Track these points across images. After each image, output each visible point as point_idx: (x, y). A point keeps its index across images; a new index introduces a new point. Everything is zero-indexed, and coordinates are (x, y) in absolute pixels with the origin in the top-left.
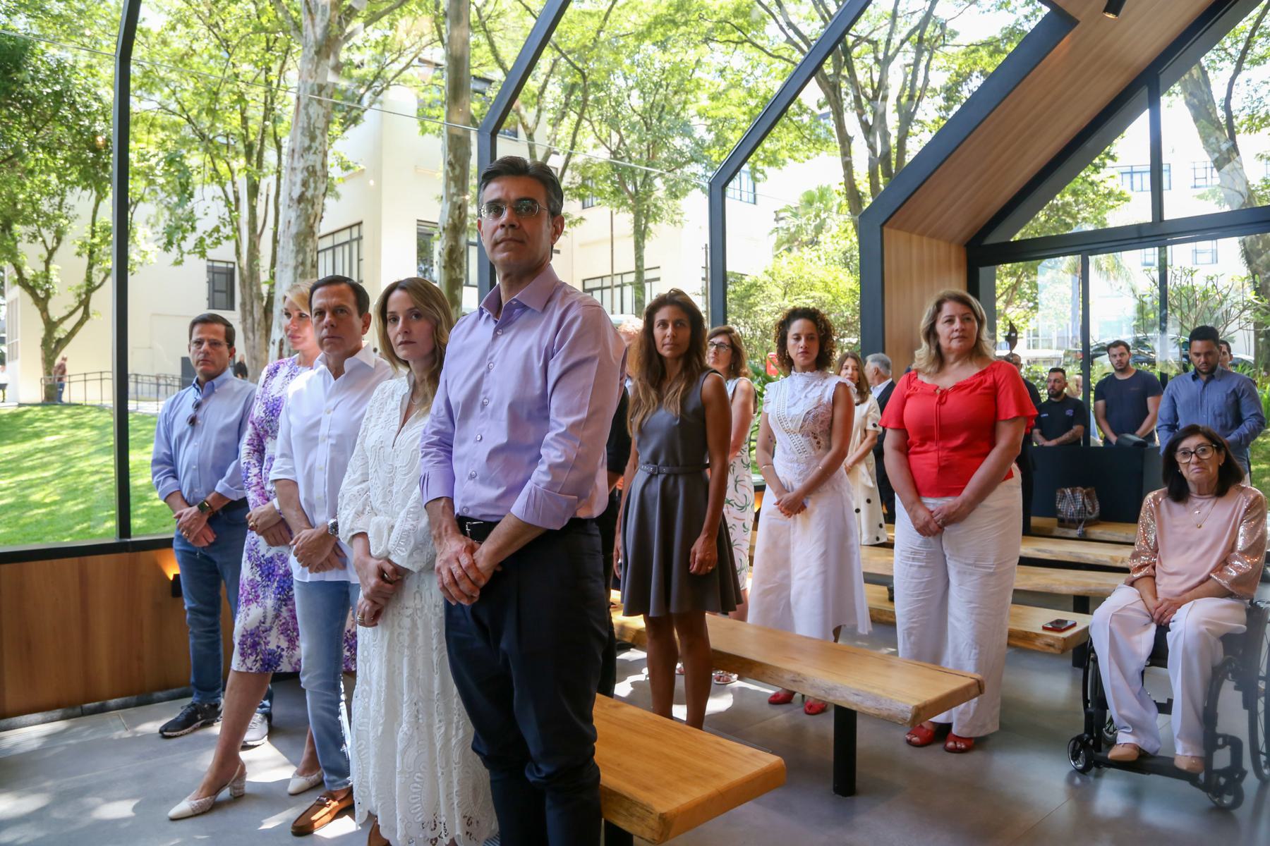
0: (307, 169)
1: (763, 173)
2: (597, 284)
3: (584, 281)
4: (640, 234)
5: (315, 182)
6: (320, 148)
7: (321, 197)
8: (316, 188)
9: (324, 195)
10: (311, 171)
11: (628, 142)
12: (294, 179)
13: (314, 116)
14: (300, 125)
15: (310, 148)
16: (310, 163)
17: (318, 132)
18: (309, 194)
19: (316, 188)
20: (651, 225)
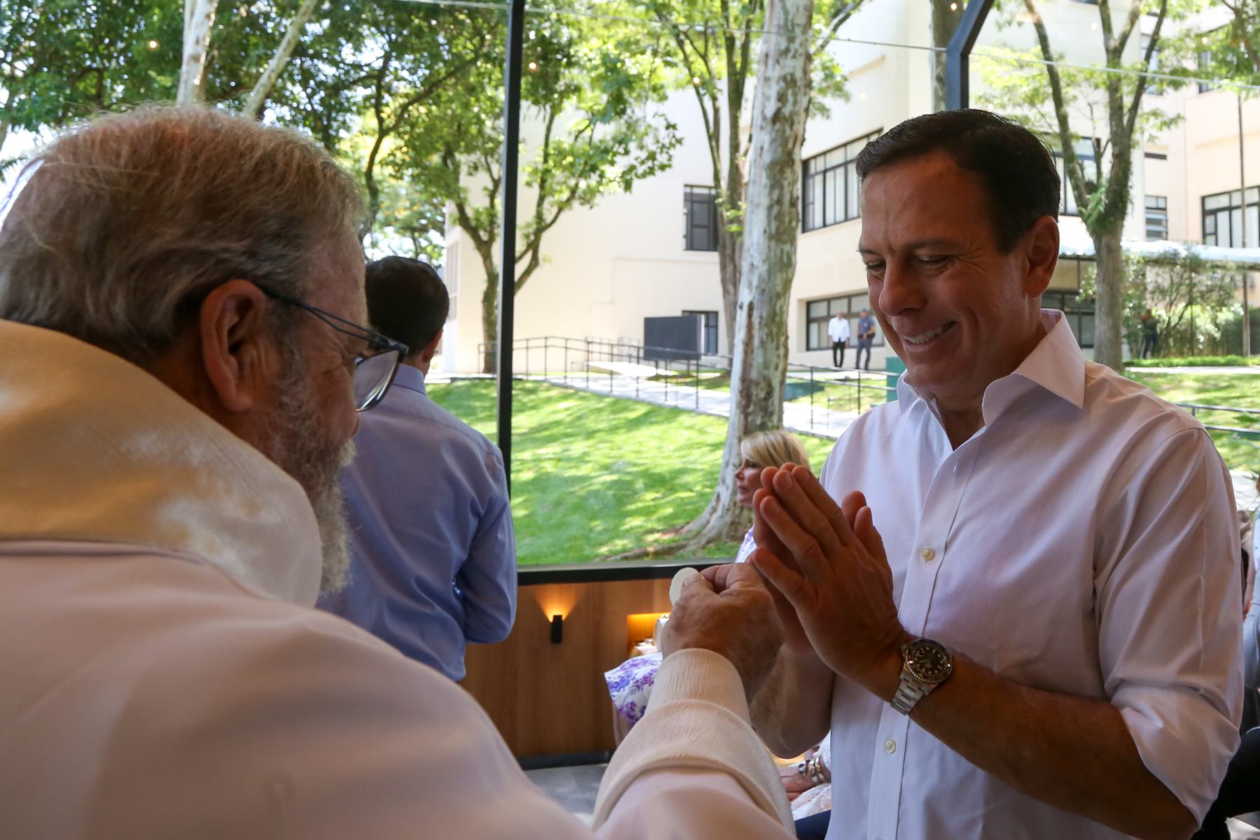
0: (784, 78)
2: (1224, 202)
3: (1203, 199)
5: (795, 95)
6: (801, 50)
7: (803, 115)
10: (789, 81)
12: (768, 92)
14: (775, 22)
15: (787, 51)
16: (788, 70)
18: (787, 111)
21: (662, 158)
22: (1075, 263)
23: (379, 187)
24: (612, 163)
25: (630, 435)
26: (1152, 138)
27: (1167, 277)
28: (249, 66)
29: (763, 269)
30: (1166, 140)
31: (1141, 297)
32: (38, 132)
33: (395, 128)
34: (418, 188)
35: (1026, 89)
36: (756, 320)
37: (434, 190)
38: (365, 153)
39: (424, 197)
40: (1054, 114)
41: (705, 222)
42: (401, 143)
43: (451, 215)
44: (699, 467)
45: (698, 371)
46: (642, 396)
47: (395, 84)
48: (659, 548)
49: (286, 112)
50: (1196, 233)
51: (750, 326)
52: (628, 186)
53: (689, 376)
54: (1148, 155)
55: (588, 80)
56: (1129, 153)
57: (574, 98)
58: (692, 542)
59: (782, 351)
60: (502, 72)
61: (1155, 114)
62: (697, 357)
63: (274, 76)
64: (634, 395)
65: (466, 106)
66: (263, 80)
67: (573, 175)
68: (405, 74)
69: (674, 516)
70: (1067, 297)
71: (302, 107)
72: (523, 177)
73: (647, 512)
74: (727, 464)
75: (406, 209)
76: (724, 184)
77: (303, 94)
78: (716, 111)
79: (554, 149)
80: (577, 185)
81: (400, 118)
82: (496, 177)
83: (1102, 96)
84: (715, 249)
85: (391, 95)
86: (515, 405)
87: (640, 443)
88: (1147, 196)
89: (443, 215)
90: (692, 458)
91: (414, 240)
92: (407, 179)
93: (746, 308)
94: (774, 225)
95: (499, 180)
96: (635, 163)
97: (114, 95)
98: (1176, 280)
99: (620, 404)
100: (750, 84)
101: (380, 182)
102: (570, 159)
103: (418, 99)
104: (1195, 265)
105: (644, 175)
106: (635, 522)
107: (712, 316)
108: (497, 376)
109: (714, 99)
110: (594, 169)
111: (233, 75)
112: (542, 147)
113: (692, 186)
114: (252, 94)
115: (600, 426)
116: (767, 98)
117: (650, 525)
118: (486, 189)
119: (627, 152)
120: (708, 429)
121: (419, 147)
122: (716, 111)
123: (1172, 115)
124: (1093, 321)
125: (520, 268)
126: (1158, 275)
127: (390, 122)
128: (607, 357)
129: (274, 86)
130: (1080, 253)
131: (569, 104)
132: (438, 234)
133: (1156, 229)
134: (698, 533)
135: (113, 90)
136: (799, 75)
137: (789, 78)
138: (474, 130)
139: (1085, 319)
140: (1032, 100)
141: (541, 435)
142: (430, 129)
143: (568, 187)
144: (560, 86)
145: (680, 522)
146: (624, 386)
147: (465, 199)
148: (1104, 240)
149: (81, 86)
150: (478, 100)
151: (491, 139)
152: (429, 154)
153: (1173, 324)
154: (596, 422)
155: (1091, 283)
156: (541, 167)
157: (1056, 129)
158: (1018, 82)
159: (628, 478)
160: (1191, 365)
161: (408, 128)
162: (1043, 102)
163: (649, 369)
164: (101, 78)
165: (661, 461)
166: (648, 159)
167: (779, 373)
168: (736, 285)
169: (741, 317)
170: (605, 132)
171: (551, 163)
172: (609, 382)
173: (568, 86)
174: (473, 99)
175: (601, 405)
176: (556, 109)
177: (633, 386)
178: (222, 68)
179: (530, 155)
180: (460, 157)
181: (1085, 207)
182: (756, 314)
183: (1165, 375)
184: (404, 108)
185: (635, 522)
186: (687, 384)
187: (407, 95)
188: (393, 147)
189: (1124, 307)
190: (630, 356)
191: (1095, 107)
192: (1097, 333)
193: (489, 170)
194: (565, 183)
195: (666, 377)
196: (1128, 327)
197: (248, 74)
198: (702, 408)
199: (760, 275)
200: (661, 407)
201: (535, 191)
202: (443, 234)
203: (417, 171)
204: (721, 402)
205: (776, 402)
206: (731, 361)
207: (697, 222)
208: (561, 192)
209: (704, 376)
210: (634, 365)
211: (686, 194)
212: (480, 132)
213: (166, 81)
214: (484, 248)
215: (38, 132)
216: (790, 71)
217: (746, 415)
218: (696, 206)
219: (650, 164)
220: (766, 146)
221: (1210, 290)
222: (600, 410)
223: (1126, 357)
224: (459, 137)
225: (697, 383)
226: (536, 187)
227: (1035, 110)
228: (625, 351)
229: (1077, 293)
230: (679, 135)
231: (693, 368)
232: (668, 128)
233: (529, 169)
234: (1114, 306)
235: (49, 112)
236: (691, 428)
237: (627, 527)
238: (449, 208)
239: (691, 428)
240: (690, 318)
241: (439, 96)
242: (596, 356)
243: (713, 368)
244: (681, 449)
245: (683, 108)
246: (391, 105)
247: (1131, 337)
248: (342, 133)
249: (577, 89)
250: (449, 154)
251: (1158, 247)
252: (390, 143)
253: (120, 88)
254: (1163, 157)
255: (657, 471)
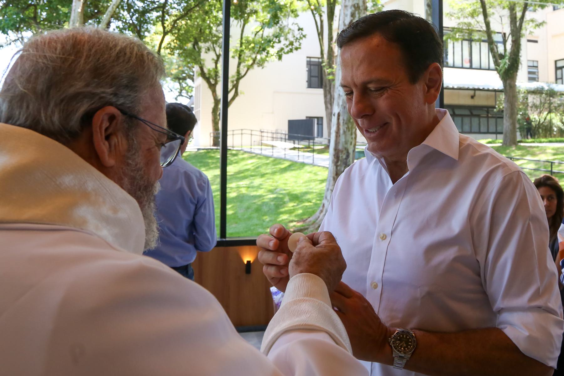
0: (354, 6)
3: (556, 62)
12: (346, 13)
21: (296, 44)
22: (494, 93)
23: (164, 59)
24: (273, 47)
25: (282, 175)
26: (531, 33)
27: (539, 99)
28: (103, 3)
30: (538, 33)
31: (526, 109)
32: (8, 34)
33: (171, 31)
34: (181, 59)
35: (470, 10)
36: (341, 121)
37: (189, 60)
38: (157, 43)
39: (184, 63)
40: (483, 21)
41: (317, 75)
42: (173, 38)
43: (197, 72)
44: (314, 191)
45: (313, 145)
46: (287, 157)
47: (171, 10)
48: (296, 229)
49: (120, 24)
50: (553, 78)
51: (338, 124)
52: (280, 58)
53: (309, 148)
54: (529, 41)
55: (261, 7)
56: (520, 40)
57: (254, 16)
58: (311, 227)
59: (353, 136)
60: (221, 4)
61: (532, 21)
62: (313, 139)
63: (115, 7)
64: (283, 157)
65: (204, 20)
66: (110, 9)
67: (254, 52)
68: (175, 6)
69: (303, 214)
70: (490, 109)
71: (127, 22)
72: (231, 54)
73: (290, 212)
74: (328, 189)
75: (176, 69)
76: (325, 56)
77: (128, 16)
78: (322, 22)
79: (245, 40)
80: (256, 57)
81: (173, 27)
82: (218, 54)
83: (506, 12)
84: (321, 87)
85: (169, 16)
86: (228, 161)
87: (286, 179)
88: (528, 60)
89: (193, 72)
90: (311, 187)
91: (180, 84)
92: (176, 55)
95: (220, 55)
96: (283, 47)
97: (42, 17)
98: (543, 101)
99: (277, 161)
100: (338, 9)
101: (164, 56)
102: (252, 45)
103: (181, 17)
104: (552, 94)
105: (288, 52)
106: (284, 217)
107: (320, 119)
108: (220, 148)
109: (321, 16)
110: (264, 50)
111: (96, 7)
112: (240, 40)
113: (310, 58)
114: (105, 16)
115: (268, 171)
116: (346, 15)
117: (291, 219)
118: (213, 59)
119: (280, 42)
120: (318, 173)
121: (182, 39)
122: (322, 22)
123: (540, 21)
124: (503, 121)
125: (230, 96)
126: (534, 98)
127: (168, 28)
128: (270, 139)
129: (115, 12)
130: (496, 88)
131: (252, 19)
132: (191, 81)
133: (533, 76)
134: (314, 223)
135: (41, 14)
136: (361, 4)
137: (356, 5)
138: (207, 31)
139: (499, 120)
140: (473, 15)
141: (241, 175)
142: (187, 31)
143: (252, 58)
144: (248, 10)
145: (305, 217)
146: (279, 152)
147: (204, 64)
148: (508, 82)
149: (27, 13)
150: (209, 18)
151: (215, 36)
152: (186, 43)
153: (541, 122)
154: (265, 169)
155: (502, 103)
156: (239, 49)
157: (484, 28)
158: (466, 6)
159: (281, 196)
160: (550, 142)
161: (177, 31)
162: (478, 16)
163: (290, 145)
164: (36, 9)
165: (296, 188)
166: (289, 45)
167: (352, 146)
168: (331, 104)
169: (334, 120)
170: (269, 32)
171: (244, 47)
172: (271, 150)
173: (251, 11)
174: (207, 17)
175: (268, 162)
176: (246, 21)
177: (283, 152)
178: (91, 3)
179: (234, 43)
180: (201, 44)
181: (499, 66)
182: (341, 118)
183: (538, 147)
184: (175, 22)
185: (284, 217)
186: (308, 151)
187: (176, 16)
188: (170, 40)
189: (517, 114)
190: (281, 138)
191: (503, 18)
192: (505, 126)
193: (215, 50)
194: (250, 56)
195: (299, 148)
196: (519, 124)
197: (103, 6)
198: (316, 163)
199: (343, 100)
200: (296, 162)
201: (236, 60)
202: (193, 80)
203: (181, 51)
204: (324, 160)
205: (351, 160)
206: (329, 141)
207: (312, 74)
208: (248, 60)
209: (317, 148)
210: (283, 142)
211: (307, 61)
212: (210, 32)
213: (65, 10)
214: (213, 87)
215: (8, 34)
216: (357, 2)
217: (337, 166)
218: (312, 67)
219: (290, 47)
221: (560, 106)
222: (267, 164)
223: (519, 138)
224: (201, 35)
225: (313, 151)
226: (237, 58)
227: (474, 20)
228: (279, 136)
229: (495, 108)
230: (304, 33)
231: (311, 144)
232: (299, 29)
233: (233, 50)
234: (513, 114)
235: (12, 25)
236: (310, 172)
237: (280, 219)
238: (196, 68)
239: (310, 172)
240: (310, 120)
241: (191, 16)
242: (265, 138)
243: (321, 144)
244: (306, 182)
245: (306, 21)
246: (169, 20)
247: (521, 129)
248: (146, 34)
249: (256, 12)
250: (196, 43)
251: (534, 85)
252: (169, 38)
253: (44, 14)
254: (536, 42)
255: (295, 193)
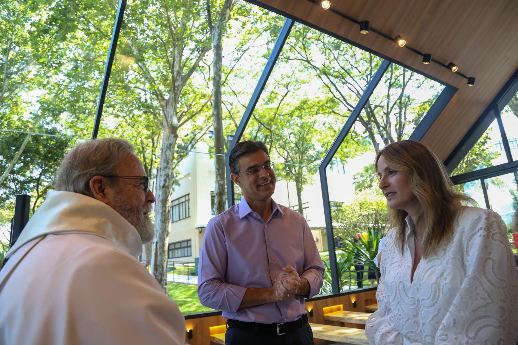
0: (166, 175)
1: (345, 161)
4: (299, 190)
5: (169, 180)
8: (169, 182)
9: (172, 184)
10: (167, 176)
11: (291, 154)
13: (168, 155)
15: (167, 167)
16: (167, 173)
17: (170, 161)
18: (167, 184)
19: (169, 182)
20: (303, 186)
29: (160, 231)
36: (158, 247)
51: (156, 249)
93: (155, 243)
94: (163, 218)
167: (165, 263)
182: (158, 245)
220: (161, 195)
